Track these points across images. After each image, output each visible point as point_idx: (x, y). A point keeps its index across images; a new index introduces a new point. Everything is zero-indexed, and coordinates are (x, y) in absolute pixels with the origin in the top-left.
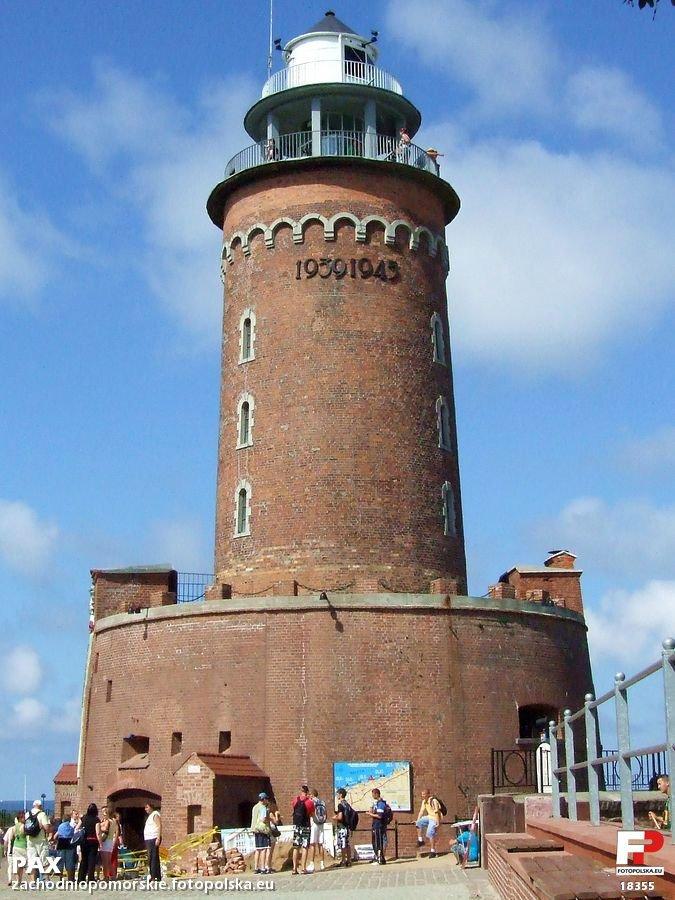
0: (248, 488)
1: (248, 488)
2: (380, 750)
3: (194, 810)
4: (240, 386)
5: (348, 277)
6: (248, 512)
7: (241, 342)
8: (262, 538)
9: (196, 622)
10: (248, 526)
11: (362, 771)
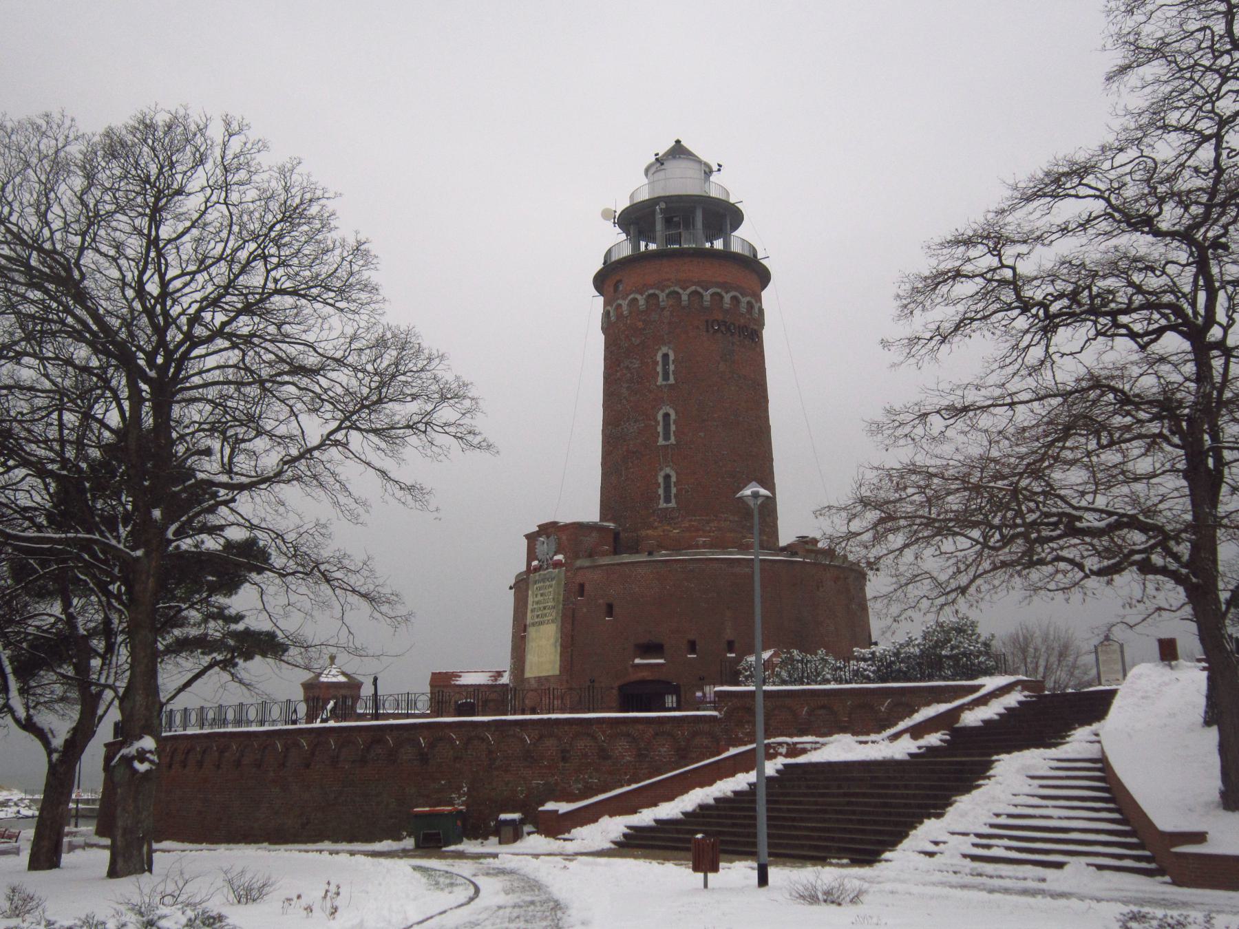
6: (674, 490)
10: (673, 501)
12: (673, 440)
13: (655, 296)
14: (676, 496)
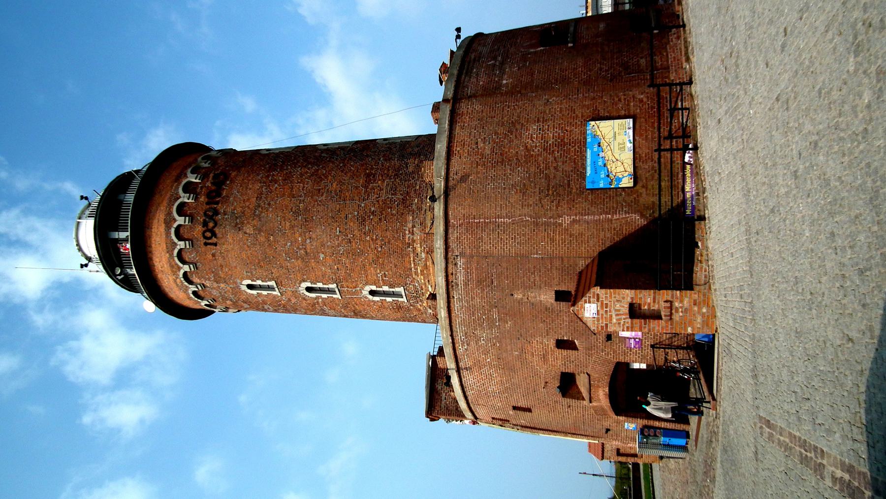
0: (368, 288)
1: (368, 288)
2: (574, 149)
3: (635, 312)
4: (295, 293)
5: (219, 207)
6: (386, 288)
7: (265, 293)
8: (404, 277)
9: (457, 322)
10: (397, 289)
11: (594, 163)
14: (391, 286)
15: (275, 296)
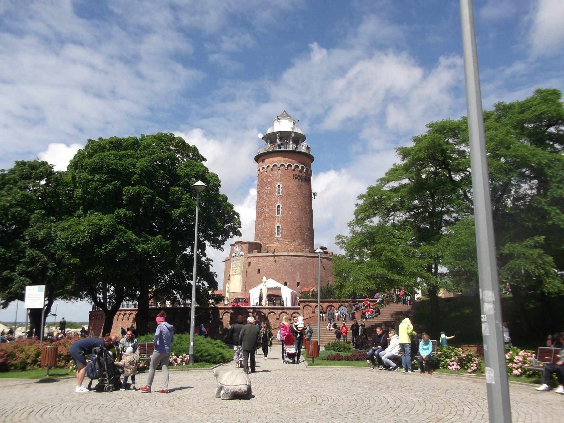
0: (280, 226)
6: (280, 231)
12: (281, 214)
13: (276, 165)
15: (275, 193)
